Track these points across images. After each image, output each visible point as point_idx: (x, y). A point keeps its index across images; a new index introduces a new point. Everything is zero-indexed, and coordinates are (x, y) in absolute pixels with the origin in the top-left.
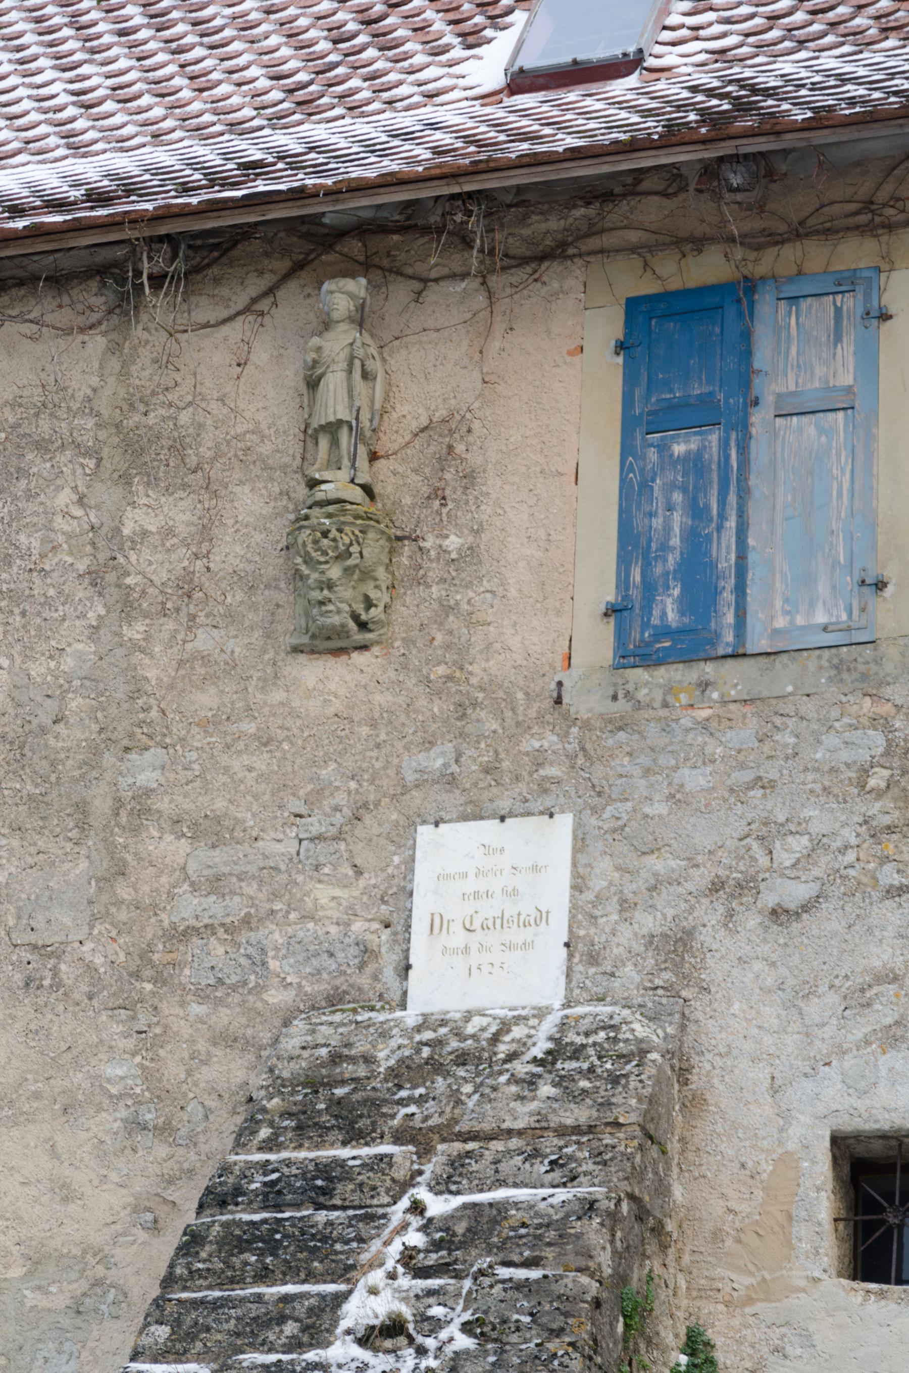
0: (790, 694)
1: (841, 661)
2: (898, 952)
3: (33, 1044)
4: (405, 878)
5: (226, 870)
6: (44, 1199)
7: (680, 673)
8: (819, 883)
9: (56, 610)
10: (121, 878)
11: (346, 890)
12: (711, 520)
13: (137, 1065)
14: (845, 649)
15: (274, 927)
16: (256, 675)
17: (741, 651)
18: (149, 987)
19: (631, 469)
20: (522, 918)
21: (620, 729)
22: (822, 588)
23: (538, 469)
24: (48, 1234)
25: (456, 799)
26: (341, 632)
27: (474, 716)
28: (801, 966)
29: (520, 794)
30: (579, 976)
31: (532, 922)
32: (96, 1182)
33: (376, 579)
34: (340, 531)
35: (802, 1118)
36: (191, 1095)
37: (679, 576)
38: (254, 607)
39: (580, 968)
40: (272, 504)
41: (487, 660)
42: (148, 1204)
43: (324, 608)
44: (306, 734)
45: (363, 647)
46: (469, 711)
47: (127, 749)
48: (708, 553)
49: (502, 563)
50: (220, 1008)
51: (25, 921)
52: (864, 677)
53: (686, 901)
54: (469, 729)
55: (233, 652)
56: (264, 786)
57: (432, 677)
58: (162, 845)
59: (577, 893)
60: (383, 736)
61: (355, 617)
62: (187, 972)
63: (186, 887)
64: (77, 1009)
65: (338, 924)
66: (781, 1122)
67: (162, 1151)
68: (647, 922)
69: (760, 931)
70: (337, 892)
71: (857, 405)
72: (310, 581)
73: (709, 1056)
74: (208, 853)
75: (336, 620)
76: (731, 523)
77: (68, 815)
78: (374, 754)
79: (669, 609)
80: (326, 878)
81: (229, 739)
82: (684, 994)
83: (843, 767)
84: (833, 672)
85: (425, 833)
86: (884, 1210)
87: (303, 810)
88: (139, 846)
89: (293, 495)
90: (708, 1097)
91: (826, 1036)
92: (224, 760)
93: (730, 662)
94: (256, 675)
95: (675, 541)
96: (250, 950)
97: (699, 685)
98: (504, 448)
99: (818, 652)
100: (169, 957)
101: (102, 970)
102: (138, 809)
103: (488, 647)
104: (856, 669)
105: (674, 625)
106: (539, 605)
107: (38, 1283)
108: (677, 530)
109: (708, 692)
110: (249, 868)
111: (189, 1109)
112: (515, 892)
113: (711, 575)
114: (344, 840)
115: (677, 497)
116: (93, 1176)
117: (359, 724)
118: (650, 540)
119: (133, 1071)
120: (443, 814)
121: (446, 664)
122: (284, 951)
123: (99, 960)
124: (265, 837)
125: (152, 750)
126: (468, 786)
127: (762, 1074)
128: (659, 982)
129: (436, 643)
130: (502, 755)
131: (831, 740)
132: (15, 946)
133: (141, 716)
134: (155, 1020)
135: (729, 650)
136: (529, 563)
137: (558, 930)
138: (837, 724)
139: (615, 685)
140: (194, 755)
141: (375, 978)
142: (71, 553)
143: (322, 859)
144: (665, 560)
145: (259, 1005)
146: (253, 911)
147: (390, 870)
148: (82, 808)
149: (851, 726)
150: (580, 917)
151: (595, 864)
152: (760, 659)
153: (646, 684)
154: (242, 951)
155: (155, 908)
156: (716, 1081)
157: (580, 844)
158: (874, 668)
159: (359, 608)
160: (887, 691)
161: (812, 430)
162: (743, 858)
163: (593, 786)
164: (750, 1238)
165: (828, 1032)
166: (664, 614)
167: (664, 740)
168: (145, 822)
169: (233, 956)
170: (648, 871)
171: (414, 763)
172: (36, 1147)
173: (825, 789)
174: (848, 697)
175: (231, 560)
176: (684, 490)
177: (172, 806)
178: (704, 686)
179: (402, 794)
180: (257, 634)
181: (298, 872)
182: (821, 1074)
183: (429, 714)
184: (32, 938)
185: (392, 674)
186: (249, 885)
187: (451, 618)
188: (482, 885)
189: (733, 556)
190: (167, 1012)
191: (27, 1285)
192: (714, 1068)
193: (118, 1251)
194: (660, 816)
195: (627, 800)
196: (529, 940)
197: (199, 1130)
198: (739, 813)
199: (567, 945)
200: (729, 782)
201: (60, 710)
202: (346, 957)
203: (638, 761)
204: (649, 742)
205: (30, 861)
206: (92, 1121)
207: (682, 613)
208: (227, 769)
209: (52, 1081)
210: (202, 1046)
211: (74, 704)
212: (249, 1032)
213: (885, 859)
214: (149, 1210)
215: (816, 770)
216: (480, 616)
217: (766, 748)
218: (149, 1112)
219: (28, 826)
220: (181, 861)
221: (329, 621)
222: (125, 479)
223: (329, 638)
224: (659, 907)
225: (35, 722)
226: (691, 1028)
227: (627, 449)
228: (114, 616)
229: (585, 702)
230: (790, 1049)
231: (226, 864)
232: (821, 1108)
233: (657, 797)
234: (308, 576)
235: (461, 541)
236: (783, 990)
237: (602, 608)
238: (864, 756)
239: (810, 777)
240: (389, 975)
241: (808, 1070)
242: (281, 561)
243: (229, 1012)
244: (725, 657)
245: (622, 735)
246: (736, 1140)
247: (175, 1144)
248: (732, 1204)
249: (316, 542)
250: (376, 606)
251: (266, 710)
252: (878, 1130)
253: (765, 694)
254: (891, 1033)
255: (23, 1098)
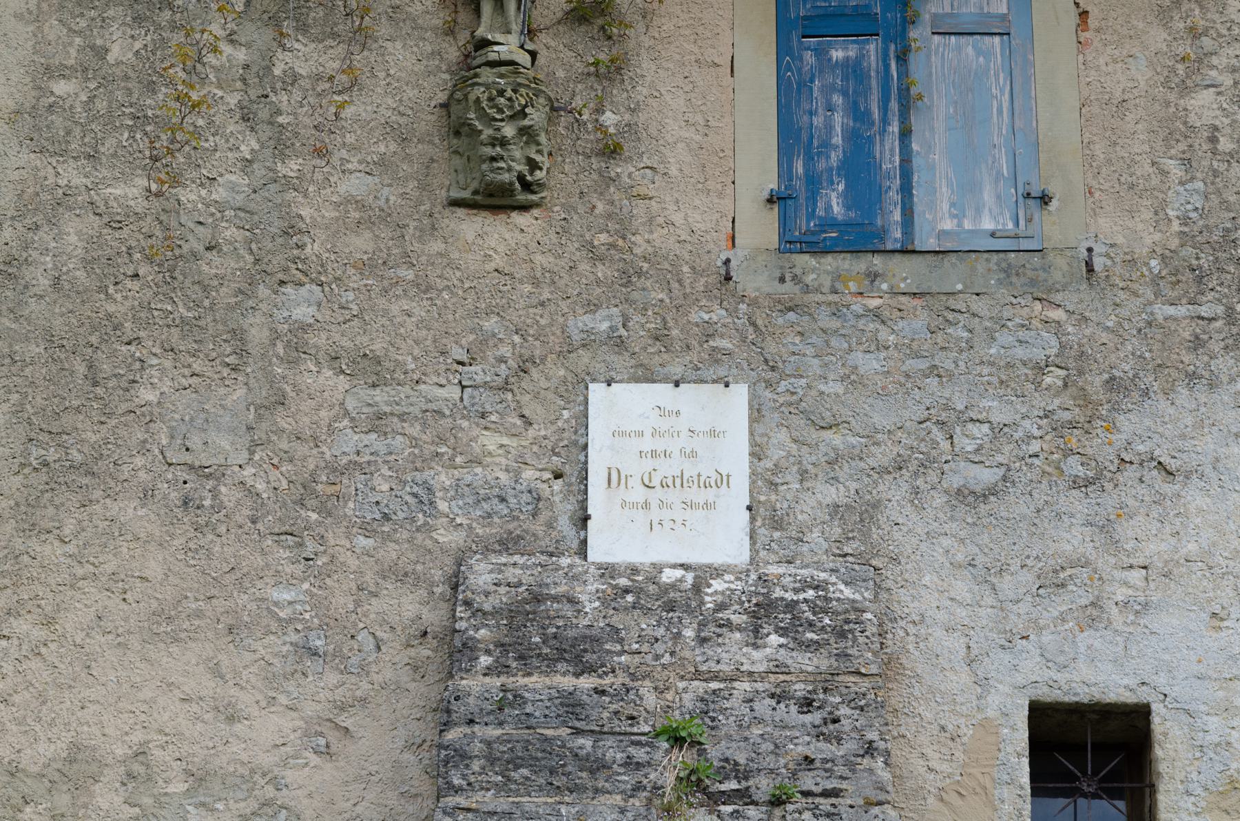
0: (960, 292)
1: (1009, 265)
2: (1087, 539)
3: (192, 562)
4: (576, 432)
5: (387, 409)
6: (206, 717)
7: (847, 262)
8: (1003, 469)
9: (207, 140)
10: (280, 408)
11: (515, 439)
12: (873, 124)
13: (306, 591)
14: (1013, 255)
15: (440, 469)
16: (413, 224)
17: (910, 248)
18: (314, 516)
19: (789, 68)
20: (702, 479)
21: (790, 309)
22: (988, 196)
23: (693, 58)
24: (212, 752)
25: (622, 362)
26: (505, 190)
27: (638, 284)
28: (991, 545)
29: (691, 362)
30: (763, 538)
31: (713, 484)
32: (263, 704)
33: (538, 144)
34: (515, 91)
35: (1000, 687)
36: (361, 625)
37: (843, 173)
38: (408, 158)
39: (763, 531)
40: (424, 62)
41: (651, 232)
42: (319, 729)
43: (496, 165)
44: (467, 286)
45: (524, 208)
46: (634, 279)
47: (282, 283)
48: (870, 154)
49: (661, 142)
50: (388, 543)
51: (179, 442)
52: (1033, 282)
53: (869, 476)
54: (635, 295)
55: (387, 200)
56: (424, 332)
57: (596, 243)
58: (321, 379)
59: (756, 461)
60: (546, 295)
61: (521, 178)
62: (351, 505)
63: (346, 422)
64: (240, 531)
65: (507, 470)
66: (979, 690)
67: (332, 678)
68: (832, 494)
69: (947, 509)
70: (505, 441)
71: (1012, 32)
72: (483, 137)
73: (902, 623)
74: (368, 392)
75: (506, 177)
76: (894, 128)
77: (225, 341)
78: (539, 311)
79: (834, 202)
80: (493, 426)
81: (386, 283)
82: (874, 563)
83: (1019, 364)
84: (1002, 275)
85: (597, 391)
86: (1078, 779)
87: (465, 358)
88: (298, 378)
89: (445, 56)
90: (904, 661)
91: (1021, 611)
92: (382, 302)
93: (898, 256)
94: (413, 224)
95: (837, 140)
96: (416, 489)
97: (868, 275)
98: (657, 36)
99: (986, 255)
100: (331, 490)
101: (265, 496)
102: (296, 344)
103: (651, 220)
104: (1025, 275)
105: (840, 218)
106: (700, 186)
107: (202, 799)
108: (839, 130)
109: (876, 283)
110: (411, 409)
111: (359, 638)
112: (693, 454)
113: (875, 174)
114: (511, 390)
115: (838, 99)
116: (260, 697)
117: (521, 282)
118: (812, 137)
119: (302, 597)
120: (613, 373)
121: (608, 232)
122: (452, 493)
123: (260, 486)
124: (428, 380)
125: (307, 286)
126: (637, 350)
127: (956, 643)
128: (847, 550)
129: (597, 211)
130: (671, 324)
131: (1004, 338)
132: (170, 465)
133: (295, 252)
134: (322, 548)
135: (898, 246)
136: (688, 146)
137: (739, 493)
138: (1009, 324)
139: (781, 268)
140: (351, 295)
141: (550, 525)
142: (220, 87)
143: (488, 408)
144: (828, 157)
145: (428, 543)
146: (416, 451)
147: (560, 424)
148: (238, 335)
149: (1023, 326)
150: (760, 483)
151: (771, 434)
152: (928, 256)
153: (813, 270)
154: (408, 489)
155: (316, 442)
156: (911, 647)
157: (756, 414)
158: (1043, 275)
159: (524, 168)
160: (1058, 298)
161: (970, 50)
162: (923, 440)
163: (766, 361)
164: (952, 798)
165: (1023, 608)
166: (829, 207)
167: (835, 324)
168: (303, 356)
169: (399, 494)
170: (827, 445)
171: (580, 322)
172: (197, 665)
173: (1002, 382)
174: (1019, 299)
175: (382, 110)
176: (845, 94)
177: (330, 342)
178: (873, 276)
179: (569, 352)
180: (412, 184)
181: (463, 417)
182: (1019, 647)
183: (592, 277)
184: (188, 458)
185: (553, 237)
186: (412, 425)
187: (612, 189)
188: (660, 445)
189: (897, 159)
190: (332, 542)
191: (190, 801)
192: (908, 634)
193: (288, 773)
194: (837, 395)
195: (802, 376)
196: (711, 500)
197: (371, 659)
198: (917, 398)
199: (749, 508)
200: (904, 368)
201: (213, 237)
202: (519, 503)
203: (810, 341)
204: (820, 323)
205: (185, 382)
206: (259, 643)
207: (848, 208)
208: (386, 312)
209: (214, 600)
210: (369, 578)
211: (228, 233)
212: (419, 568)
213: (1071, 452)
214: (321, 734)
215: (992, 364)
216: (643, 191)
217: (940, 338)
218: (319, 638)
219: (182, 348)
220: (341, 397)
221: (499, 177)
222: (274, 21)
223: (491, 195)
224: (842, 480)
225: (186, 247)
226: (884, 595)
227: (783, 49)
228: (268, 152)
229: (755, 281)
230: (985, 622)
231: (387, 403)
232: (1020, 679)
233: (831, 376)
234: (480, 131)
235: (618, 117)
236: (974, 566)
237: (766, 195)
238: (1039, 355)
239: (986, 371)
240: (565, 525)
241: (1003, 642)
242: (433, 118)
243: (397, 547)
244: (893, 252)
245: (791, 316)
246: (933, 704)
247: (346, 671)
248: (932, 764)
249: (491, 99)
250: (541, 169)
251: (424, 259)
252: (1077, 703)
253: (935, 289)
254: (1088, 613)
255: (183, 615)
